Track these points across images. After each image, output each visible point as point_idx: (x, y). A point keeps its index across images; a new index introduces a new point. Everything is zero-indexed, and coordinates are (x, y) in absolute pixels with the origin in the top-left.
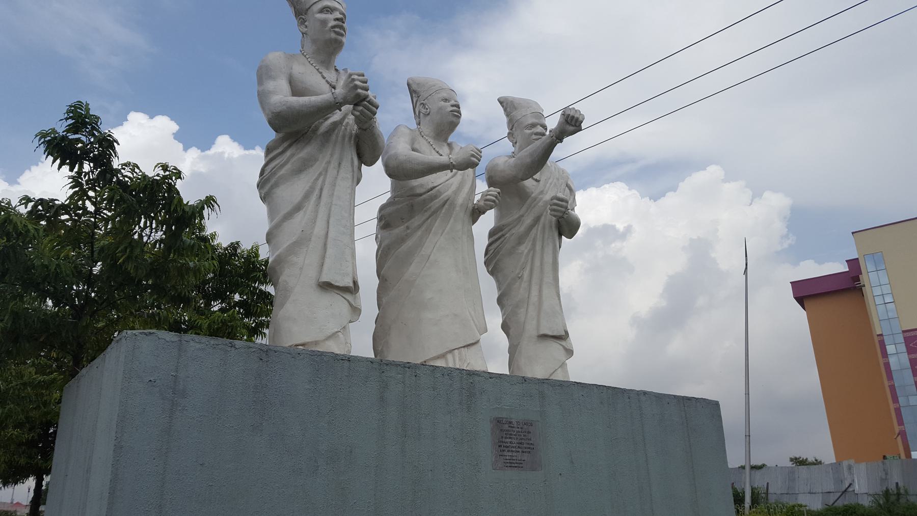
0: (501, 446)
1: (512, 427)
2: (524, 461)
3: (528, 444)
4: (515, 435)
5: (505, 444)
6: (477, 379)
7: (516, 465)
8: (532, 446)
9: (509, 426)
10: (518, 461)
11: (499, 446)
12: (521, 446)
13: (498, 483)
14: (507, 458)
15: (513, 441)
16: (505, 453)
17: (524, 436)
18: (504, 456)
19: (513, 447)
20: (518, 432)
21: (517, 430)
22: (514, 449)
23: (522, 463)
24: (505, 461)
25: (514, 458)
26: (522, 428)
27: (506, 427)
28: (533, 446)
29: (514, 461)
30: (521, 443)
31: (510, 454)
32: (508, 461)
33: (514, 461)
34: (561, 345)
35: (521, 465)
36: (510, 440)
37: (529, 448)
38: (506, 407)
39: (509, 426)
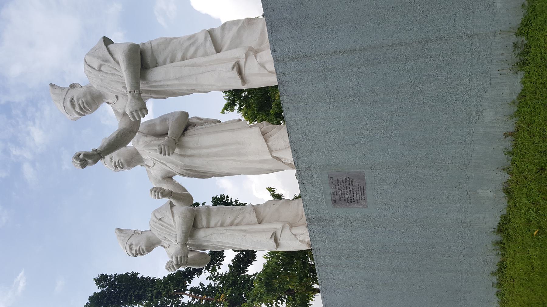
0: (351, 201)
1: (336, 193)
2: (358, 185)
3: (346, 181)
4: (342, 191)
5: (349, 199)
6: (310, 215)
7: (362, 191)
8: (347, 178)
9: (336, 195)
10: (360, 190)
11: (351, 202)
12: (348, 187)
13: (376, 205)
14: (358, 197)
15: (346, 192)
16: (355, 199)
17: (341, 184)
18: (357, 199)
19: (350, 193)
21: (337, 189)
22: (352, 192)
23: (361, 187)
24: (361, 198)
25: (358, 192)
26: (336, 186)
27: (337, 197)
28: (347, 177)
29: (360, 192)
30: (347, 187)
31: (355, 195)
32: (360, 197)
33: (360, 192)
34: (245, 63)
35: (362, 187)
37: (349, 181)
38: (324, 196)
39: (336, 195)
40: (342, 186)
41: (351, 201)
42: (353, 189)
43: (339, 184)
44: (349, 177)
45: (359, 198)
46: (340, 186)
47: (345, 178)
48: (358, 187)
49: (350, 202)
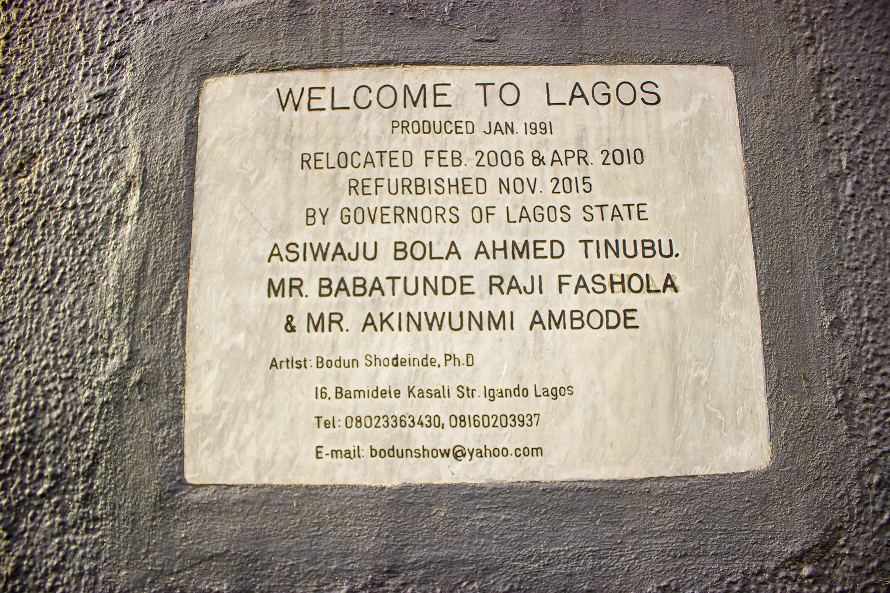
1: (443, 128)
2: (555, 393)
3: (613, 248)
5: (335, 270)
10: (479, 406)
11: (273, 289)
14: (357, 379)
17: (564, 185)
20: (500, 158)
21: (498, 143)
24: (348, 407)
25: (434, 378)
28: (674, 267)
29: (433, 406)
30: (521, 251)
33: (433, 406)
36: (405, 232)
37: (624, 283)
40: (530, 201)
41: (296, 286)
42: (497, 321)
43: (562, 171)
44: (669, 283)
45: (340, 393)
46: (529, 171)
47: (649, 248)
48: (521, 392)
49: (287, 271)
